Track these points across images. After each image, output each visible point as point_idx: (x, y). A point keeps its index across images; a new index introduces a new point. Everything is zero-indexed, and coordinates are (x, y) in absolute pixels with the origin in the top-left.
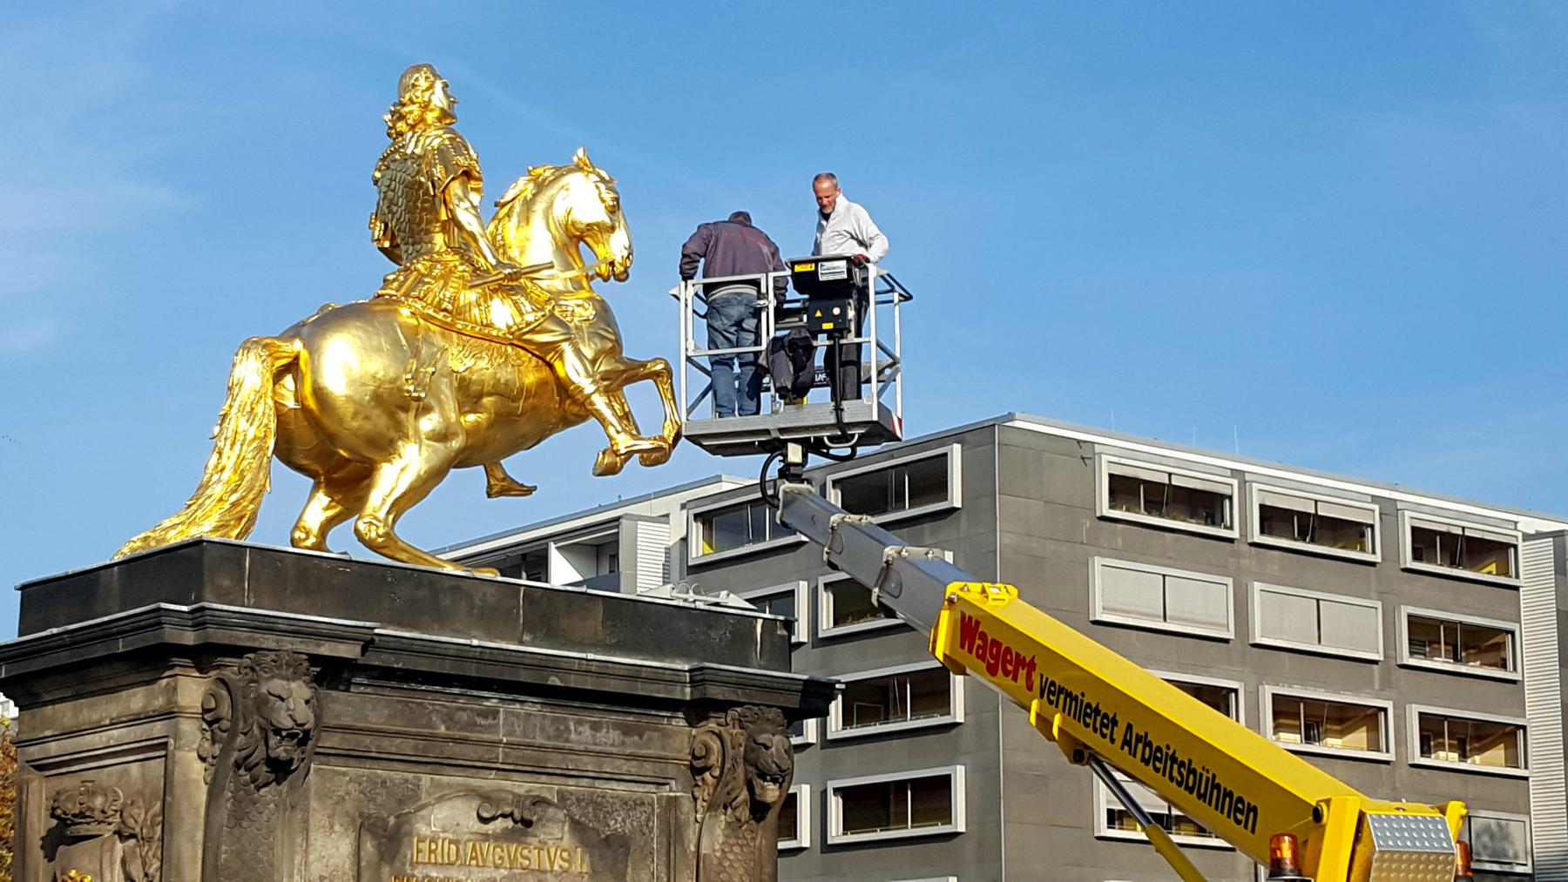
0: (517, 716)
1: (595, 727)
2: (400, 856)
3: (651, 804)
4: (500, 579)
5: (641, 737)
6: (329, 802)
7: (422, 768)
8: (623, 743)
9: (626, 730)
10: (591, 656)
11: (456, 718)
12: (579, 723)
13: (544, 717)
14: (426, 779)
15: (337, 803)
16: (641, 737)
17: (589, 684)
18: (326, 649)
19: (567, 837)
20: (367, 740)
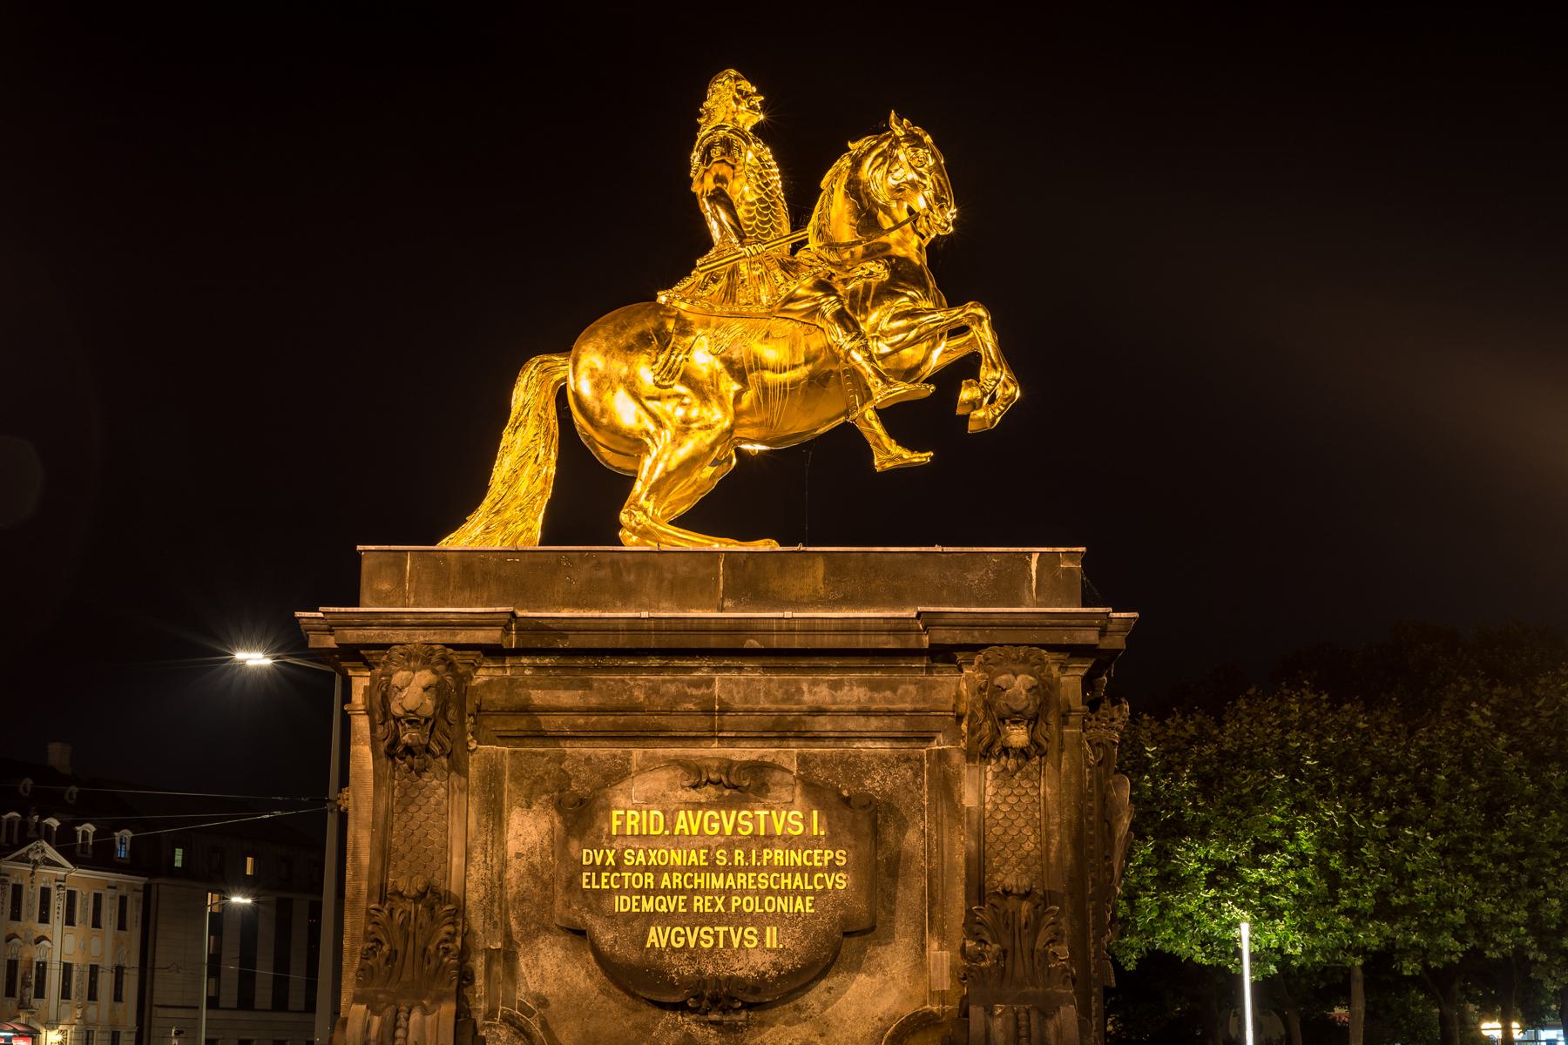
0: (737, 683)
1: (836, 686)
2: (595, 830)
3: (921, 760)
4: (779, 548)
5: (894, 690)
6: (526, 782)
7: (631, 744)
8: (872, 700)
9: (875, 686)
10: (788, 614)
11: (663, 689)
12: (814, 683)
13: (770, 681)
14: (637, 754)
15: (535, 783)
16: (894, 690)
17: (797, 642)
18: (462, 637)
19: (798, 800)
20: (560, 720)
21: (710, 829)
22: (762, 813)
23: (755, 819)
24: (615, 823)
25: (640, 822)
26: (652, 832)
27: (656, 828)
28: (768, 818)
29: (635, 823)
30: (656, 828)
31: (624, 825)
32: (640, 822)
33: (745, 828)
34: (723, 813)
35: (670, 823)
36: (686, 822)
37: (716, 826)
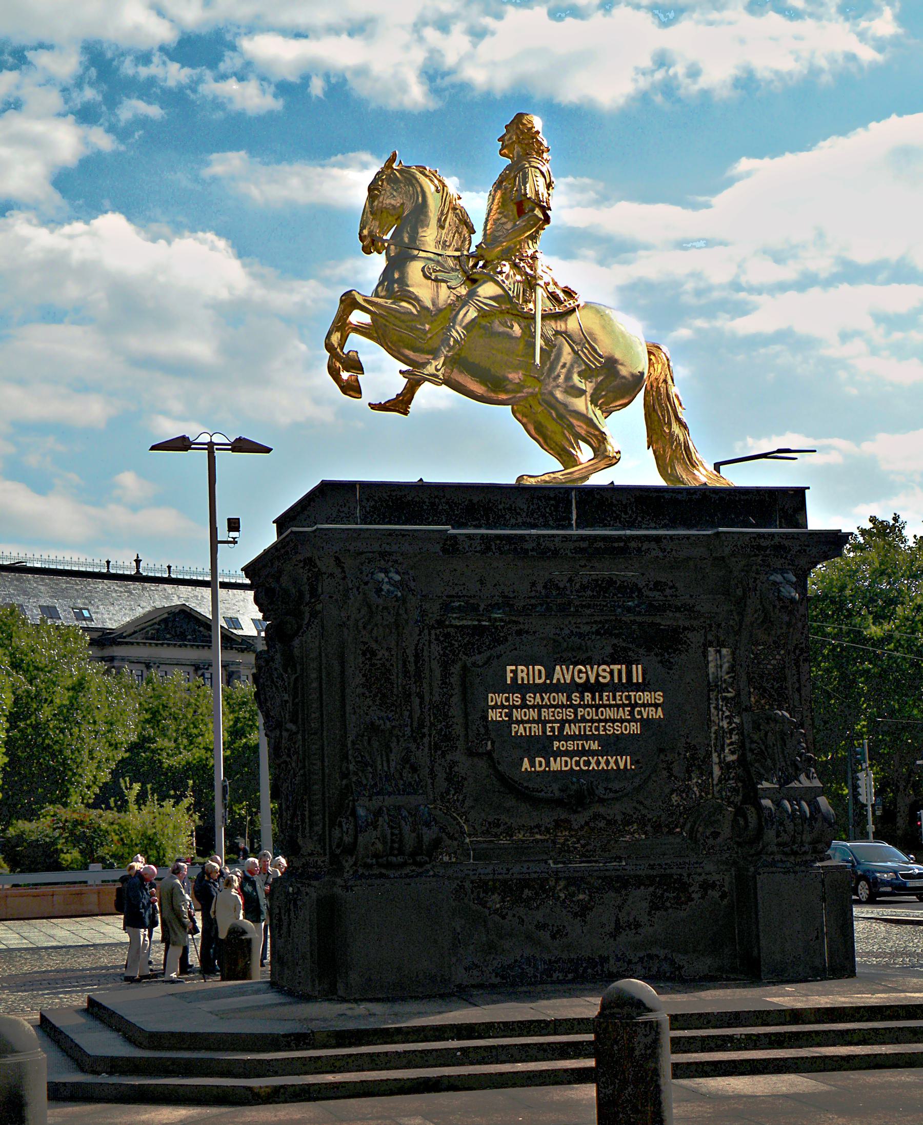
21: (580, 678)
22: (616, 667)
23: (611, 673)
24: (510, 675)
25: (528, 674)
26: (537, 681)
27: (540, 678)
28: (620, 671)
29: (524, 675)
30: (540, 678)
31: (515, 679)
32: (528, 674)
33: (604, 677)
34: (588, 667)
35: (550, 675)
36: (562, 674)
37: (583, 676)
